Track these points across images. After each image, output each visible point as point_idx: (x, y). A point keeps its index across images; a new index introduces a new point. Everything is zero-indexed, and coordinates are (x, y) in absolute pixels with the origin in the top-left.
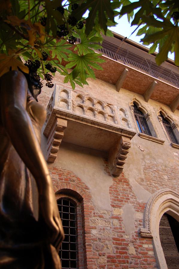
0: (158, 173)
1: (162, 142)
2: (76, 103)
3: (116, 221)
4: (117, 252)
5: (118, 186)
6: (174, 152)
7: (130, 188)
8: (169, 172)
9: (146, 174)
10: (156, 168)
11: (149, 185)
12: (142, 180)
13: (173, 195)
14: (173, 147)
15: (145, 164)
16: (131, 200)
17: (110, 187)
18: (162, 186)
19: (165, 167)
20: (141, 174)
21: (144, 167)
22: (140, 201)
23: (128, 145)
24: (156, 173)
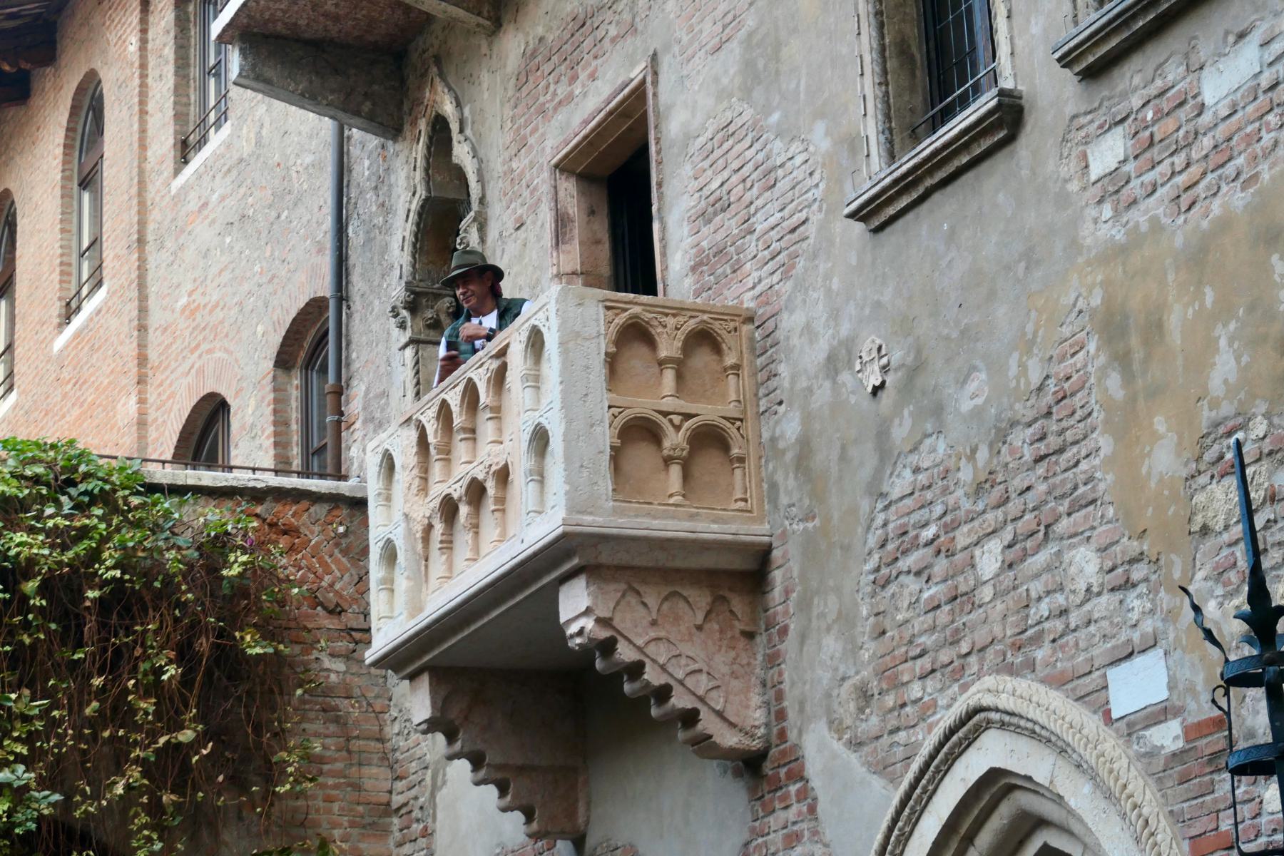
0: (950, 554)
5: (767, 831)
7: (812, 810)
8: (1018, 483)
9: (887, 624)
10: (938, 509)
11: (893, 722)
12: (864, 696)
13: (1003, 725)
14: (1093, 74)
15: (885, 524)
19: (991, 446)
20: (853, 649)
21: (876, 557)
23: (578, 640)
24: (941, 566)
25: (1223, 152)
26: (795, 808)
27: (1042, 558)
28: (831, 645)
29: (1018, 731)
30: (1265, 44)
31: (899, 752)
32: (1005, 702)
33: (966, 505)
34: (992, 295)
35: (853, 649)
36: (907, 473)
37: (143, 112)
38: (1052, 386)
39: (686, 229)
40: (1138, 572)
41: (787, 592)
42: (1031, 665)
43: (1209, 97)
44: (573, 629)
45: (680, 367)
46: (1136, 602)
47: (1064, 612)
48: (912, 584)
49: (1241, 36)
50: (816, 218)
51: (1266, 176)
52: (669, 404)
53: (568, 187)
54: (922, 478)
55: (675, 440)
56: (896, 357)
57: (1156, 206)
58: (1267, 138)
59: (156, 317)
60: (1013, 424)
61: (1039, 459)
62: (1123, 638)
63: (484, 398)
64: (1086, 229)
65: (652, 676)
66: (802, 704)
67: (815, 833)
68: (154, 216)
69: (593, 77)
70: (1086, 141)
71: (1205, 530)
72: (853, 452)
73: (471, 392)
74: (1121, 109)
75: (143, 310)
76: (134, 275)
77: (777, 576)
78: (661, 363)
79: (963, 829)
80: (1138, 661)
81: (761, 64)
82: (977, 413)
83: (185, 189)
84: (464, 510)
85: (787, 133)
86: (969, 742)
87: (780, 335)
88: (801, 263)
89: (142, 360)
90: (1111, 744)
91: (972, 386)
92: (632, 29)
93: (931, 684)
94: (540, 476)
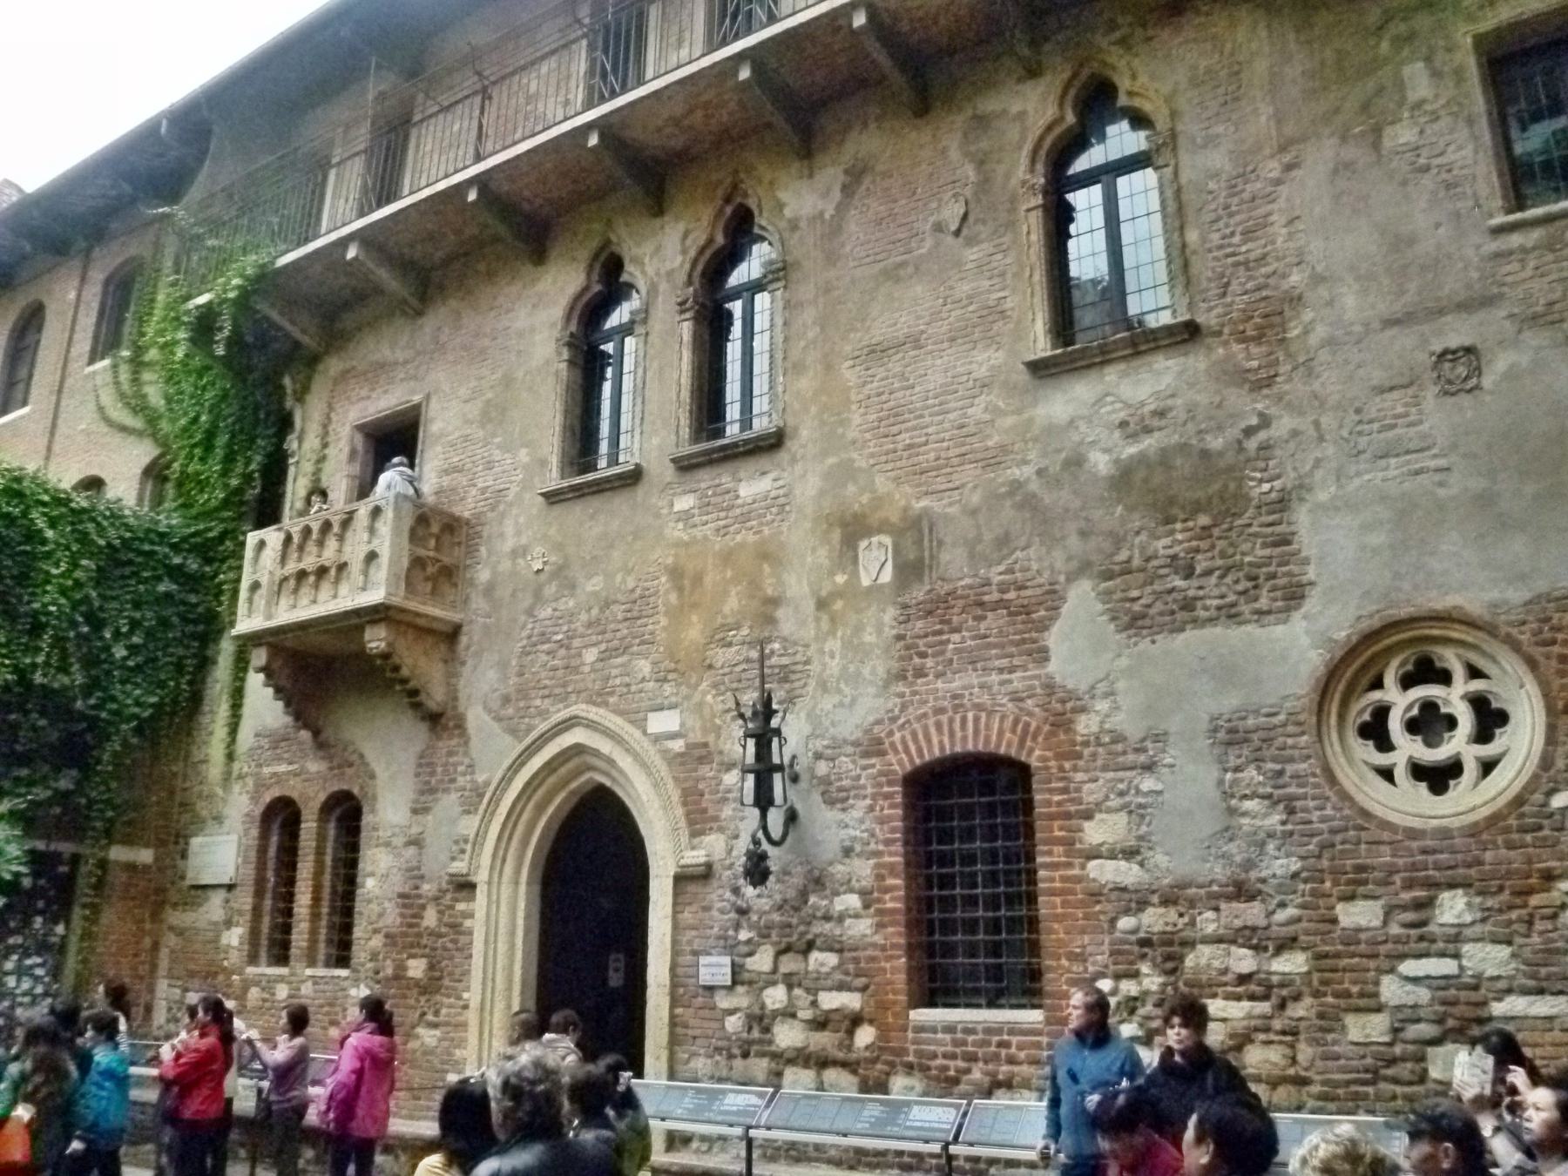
0: (568, 648)
1: (634, 477)
2: (279, 574)
3: (412, 850)
4: (402, 925)
6: (685, 493)
7: (466, 743)
8: (612, 626)
10: (565, 628)
12: (506, 700)
13: (587, 726)
16: (461, 781)
17: (421, 757)
18: (566, 699)
22: (481, 778)
24: (562, 652)
25: (745, 518)
26: (454, 742)
27: (619, 660)
28: (492, 675)
29: (596, 730)
30: (775, 480)
31: (523, 727)
32: (591, 716)
33: (581, 630)
34: (611, 546)
35: (505, 678)
36: (549, 610)
37: (73, 330)
38: (638, 591)
39: (433, 475)
40: (670, 676)
41: (468, 648)
42: (606, 704)
43: (742, 493)
44: (373, 645)
45: (438, 538)
46: (668, 689)
47: (628, 685)
48: (544, 658)
49: (764, 473)
50: (514, 489)
51: (766, 530)
52: (431, 554)
53: (359, 440)
54: (557, 614)
55: (431, 570)
56: (553, 559)
57: (708, 530)
58: (769, 517)
59: (62, 428)
60: (615, 602)
61: (626, 619)
62: (659, 701)
63: (336, 529)
64: (667, 531)
65: (405, 672)
66: (469, 697)
67: (466, 754)
68: (69, 382)
69: (386, 392)
70: (674, 495)
71: (710, 667)
72: (520, 595)
73: (327, 526)
74: (695, 486)
75: (54, 425)
76: (52, 406)
77: (464, 639)
78: (431, 535)
79: (555, 764)
80: (666, 712)
81: (493, 414)
82: (595, 594)
83: (94, 373)
84: (312, 579)
85: (505, 448)
86: (567, 729)
87: (485, 534)
88: (501, 507)
89: (49, 449)
90: (646, 743)
91: (595, 580)
92: (415, 378)
93: (547, 701)
94: (366, 573)
